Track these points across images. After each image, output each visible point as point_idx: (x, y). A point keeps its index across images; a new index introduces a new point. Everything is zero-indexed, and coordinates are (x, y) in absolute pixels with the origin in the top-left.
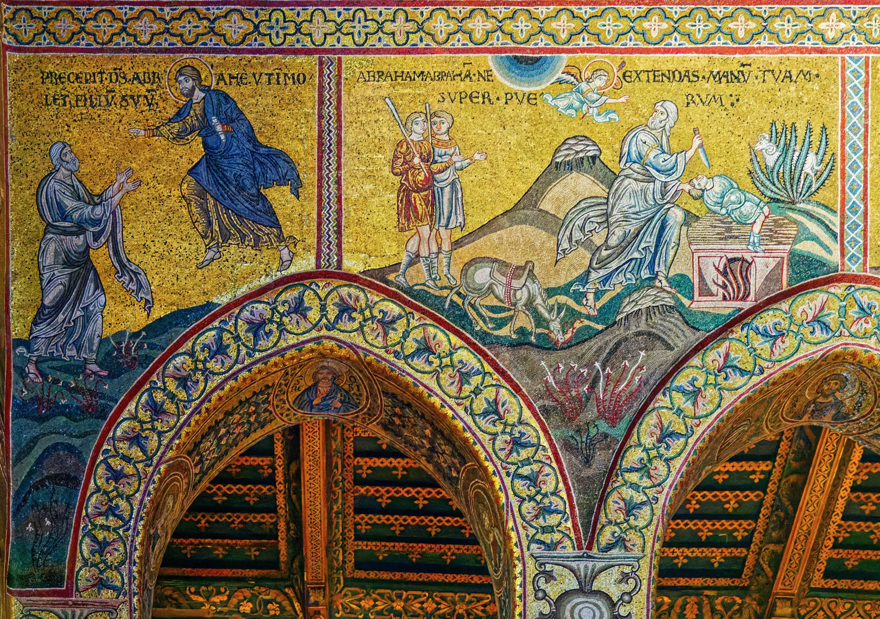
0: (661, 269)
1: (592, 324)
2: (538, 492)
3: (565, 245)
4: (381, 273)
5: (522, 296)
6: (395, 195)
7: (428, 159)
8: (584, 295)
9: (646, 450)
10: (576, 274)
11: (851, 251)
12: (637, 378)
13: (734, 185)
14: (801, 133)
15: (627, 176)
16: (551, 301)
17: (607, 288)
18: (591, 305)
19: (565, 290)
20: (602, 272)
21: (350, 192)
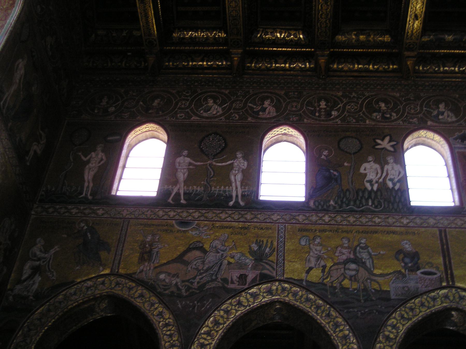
0: (219, 276)
1: (196, 291)
2: (172, 340)
3: (190, 269)
4: (130, 275)
5: (174, 282)
6: (139, 254)
7: (151, 245)
8: (194, 283)
9: (210, 328)
10: (192, 277)
11: (278, 273)
12: (208, 307)
13: (243, 255)
14: (265, 242)
15: (211, 252)
16: (183, 284)
17: (201, 281)
18: (195, 285)
19: (188, 281)
20: (200, 277)
21: (126, 253)
